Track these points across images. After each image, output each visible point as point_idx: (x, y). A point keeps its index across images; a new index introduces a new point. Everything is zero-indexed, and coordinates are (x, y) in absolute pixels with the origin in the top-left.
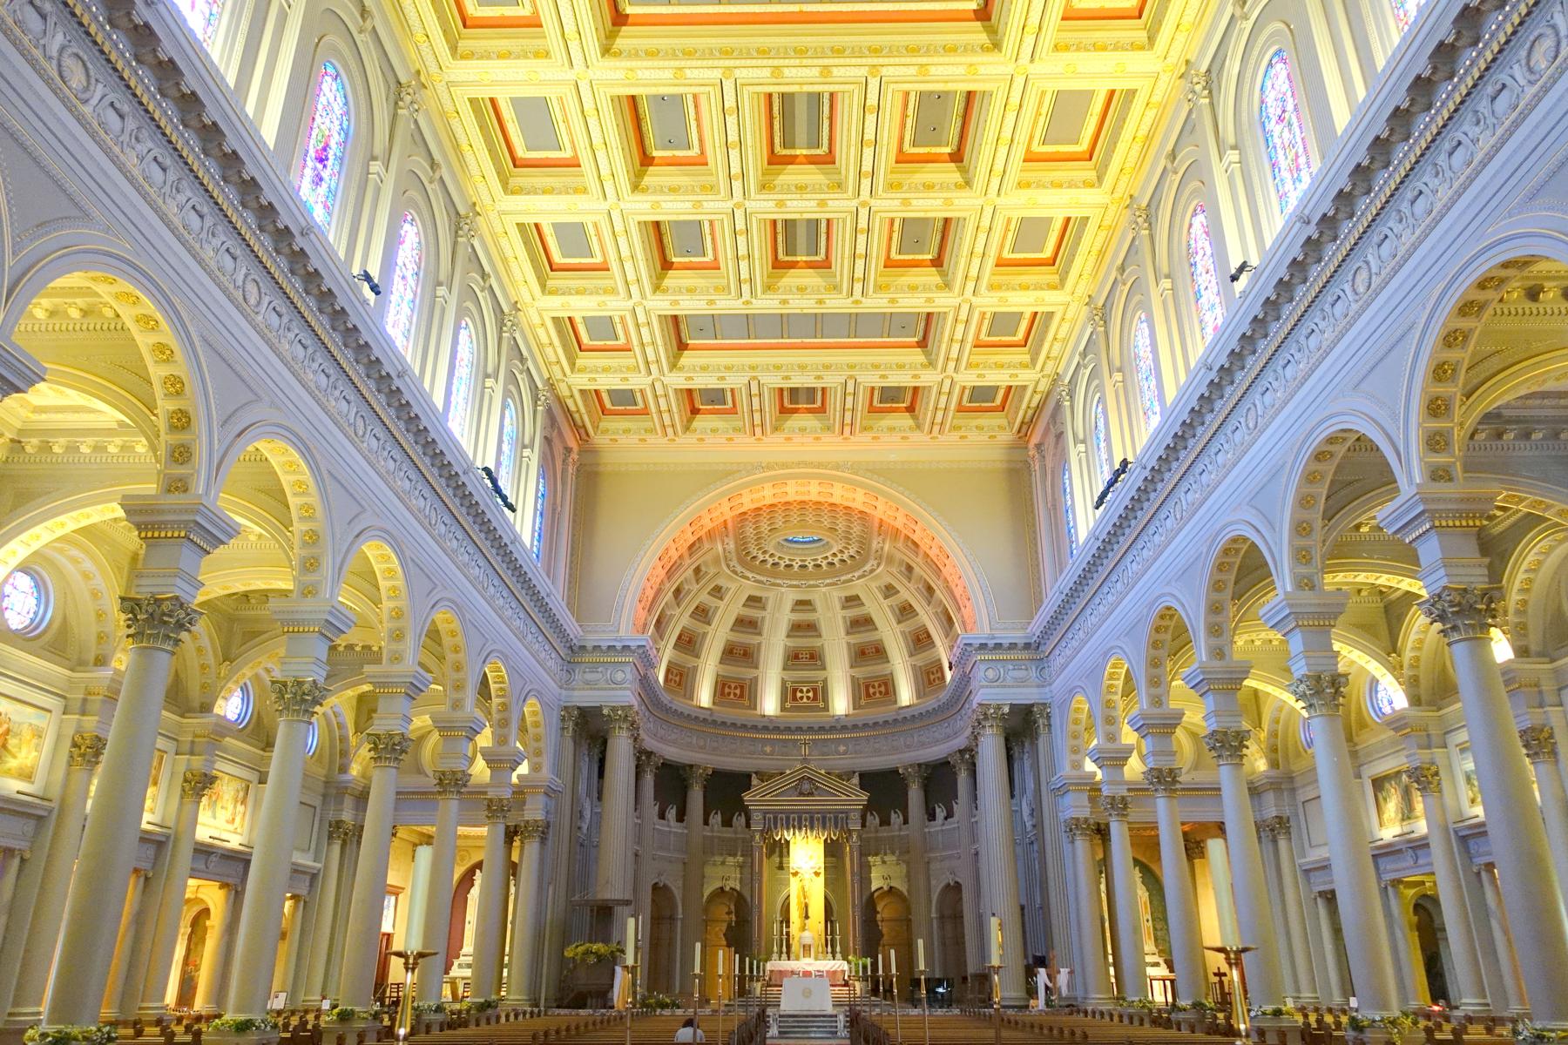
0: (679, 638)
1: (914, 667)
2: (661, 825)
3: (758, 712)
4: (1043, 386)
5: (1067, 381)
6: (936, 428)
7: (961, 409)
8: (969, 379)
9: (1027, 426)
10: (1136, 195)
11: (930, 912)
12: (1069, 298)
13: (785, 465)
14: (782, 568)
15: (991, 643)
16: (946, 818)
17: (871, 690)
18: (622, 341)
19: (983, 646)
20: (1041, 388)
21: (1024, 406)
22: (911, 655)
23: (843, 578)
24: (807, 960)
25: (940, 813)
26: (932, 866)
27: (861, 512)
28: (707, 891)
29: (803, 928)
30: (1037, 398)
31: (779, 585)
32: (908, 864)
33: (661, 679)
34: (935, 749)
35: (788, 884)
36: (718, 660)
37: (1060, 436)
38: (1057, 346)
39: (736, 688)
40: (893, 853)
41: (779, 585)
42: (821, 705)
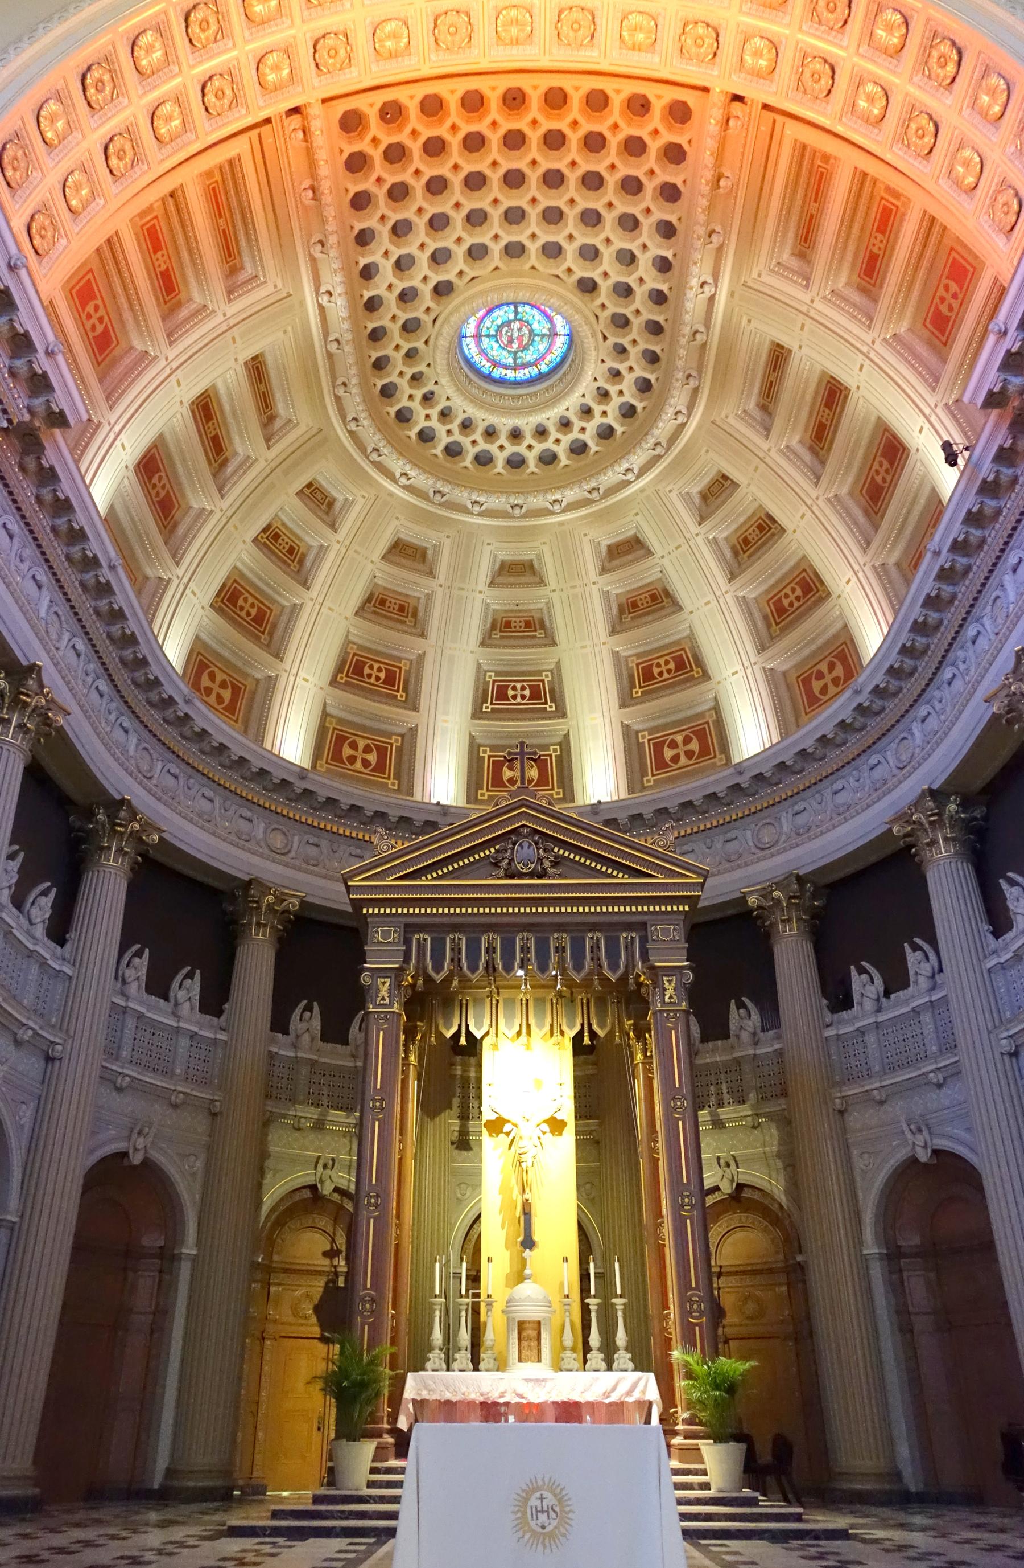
1: (770, 675)
3: (417, 797)
11: (860, 1243)
16: (887, 994)
17: (668, 753)
22: (762, 648)
24: (530, 1369)
26: (854, 1119)
28: (273, 1192)
29: (519, 1276)
32: (785, 1122)
34: (842, 830)
35: (473, 1180)
39: (367, 749)
40: (742, 1101)
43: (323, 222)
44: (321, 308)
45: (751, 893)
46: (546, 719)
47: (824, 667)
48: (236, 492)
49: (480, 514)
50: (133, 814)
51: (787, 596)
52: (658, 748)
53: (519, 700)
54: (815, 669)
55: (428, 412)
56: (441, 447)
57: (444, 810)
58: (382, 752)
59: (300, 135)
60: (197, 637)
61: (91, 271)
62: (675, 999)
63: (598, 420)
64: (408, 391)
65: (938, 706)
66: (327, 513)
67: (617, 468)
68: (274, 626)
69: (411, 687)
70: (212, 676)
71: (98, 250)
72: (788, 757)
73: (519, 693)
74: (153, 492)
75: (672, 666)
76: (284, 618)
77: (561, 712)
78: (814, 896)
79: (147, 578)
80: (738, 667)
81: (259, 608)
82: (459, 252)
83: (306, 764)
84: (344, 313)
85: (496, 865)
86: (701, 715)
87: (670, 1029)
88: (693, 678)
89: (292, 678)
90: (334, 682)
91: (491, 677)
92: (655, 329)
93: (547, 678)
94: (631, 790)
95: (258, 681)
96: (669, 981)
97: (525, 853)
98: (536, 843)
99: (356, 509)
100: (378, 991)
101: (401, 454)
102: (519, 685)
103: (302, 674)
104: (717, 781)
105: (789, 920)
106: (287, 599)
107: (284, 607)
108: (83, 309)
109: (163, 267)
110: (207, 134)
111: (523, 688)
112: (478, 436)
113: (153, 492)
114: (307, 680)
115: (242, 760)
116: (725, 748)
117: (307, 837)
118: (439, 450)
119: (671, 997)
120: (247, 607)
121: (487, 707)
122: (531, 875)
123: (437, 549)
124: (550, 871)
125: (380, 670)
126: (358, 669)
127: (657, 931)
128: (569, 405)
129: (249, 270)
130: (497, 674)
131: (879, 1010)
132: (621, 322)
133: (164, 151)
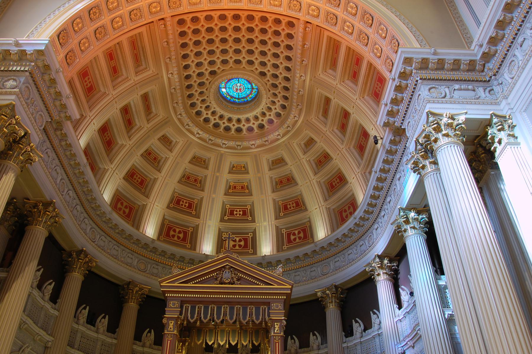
1: (328, 209)
2: (83, 328)
17: (292, 237)
22: (326, 200)
25: (358, 327)
33: (107, 196)
36: (166, 205)
39: (180, 232)
42: (251, 251)
43: (170, 52)
44: (169, 78)
45: (318, 291)
46: (248, 223)
47: (347, 208)
48: (135, 138)
49: (226, 148)
50: (86, 255)
51: (334, 182)
52: (289, 235)
53: (238, 215)
54: (344, 208)
55: (207, 112)
56: (212, 124)
57: (207, 257)
58: (185, 233)
59: (163, 26)
60: (117, 189)
61: (88, 67)
62: (279, 332)
63: (268, 117)
64: (200, 105)
65: (381, 225)
66: (169, 146)
67: (274, 134)
68: (147, 186)
69: (198, 209)
70: (122, 204)
71: (91, 61)
72: (332, 241)
73: (238, 213)
74: (105, 139)
75: (294, 205)
76: (151, 183)
77: (253, 221)
78: (342, 293)
79: (100, 168)
80: (317, 207)
81: (142, 179)
82: (218, 62)
83: (155, 238)
84: (177, 80)
85: (216, 279)
86: (304, 223)
87: (276, 343)
88: (302, 210)
89: (152, 205)
90: (168, 207)
91: (228, 207)
92: (286, 89)
93: (249, 207)
94: (278, 251)
95: (139, 206)
96: (277, 325)
97: (227, 275)
98: (231, 272)
100: (169, 325)
101: (197, 126)
102: (238, 210)
103: (156, 204)
104: (308, 248)
105: (332, 302)
106: (153, 176)
107: (151, 179)
108: (84, 79)
109: (114, 65)
110: (131, 26)
111: (240, 211)
112: (225, 121)
113: (105, 139)
114: (158, 206)
115: (130, 235)
116: (312, 236)
117: (154, 265)
118: (211, 125)
119: (277, 331)
120: (137, 178)
121: (226, 218)
122: (229, 283)
123: (209, 159)
124: (236, 282)
125: (186, 203)
126: (178, 202)
127: (274, 306)
128: (257, 112)
129: (144, 66)
130: (230, 205)
131: (362, 337)
132: (275, 86)
133: (115, 31)
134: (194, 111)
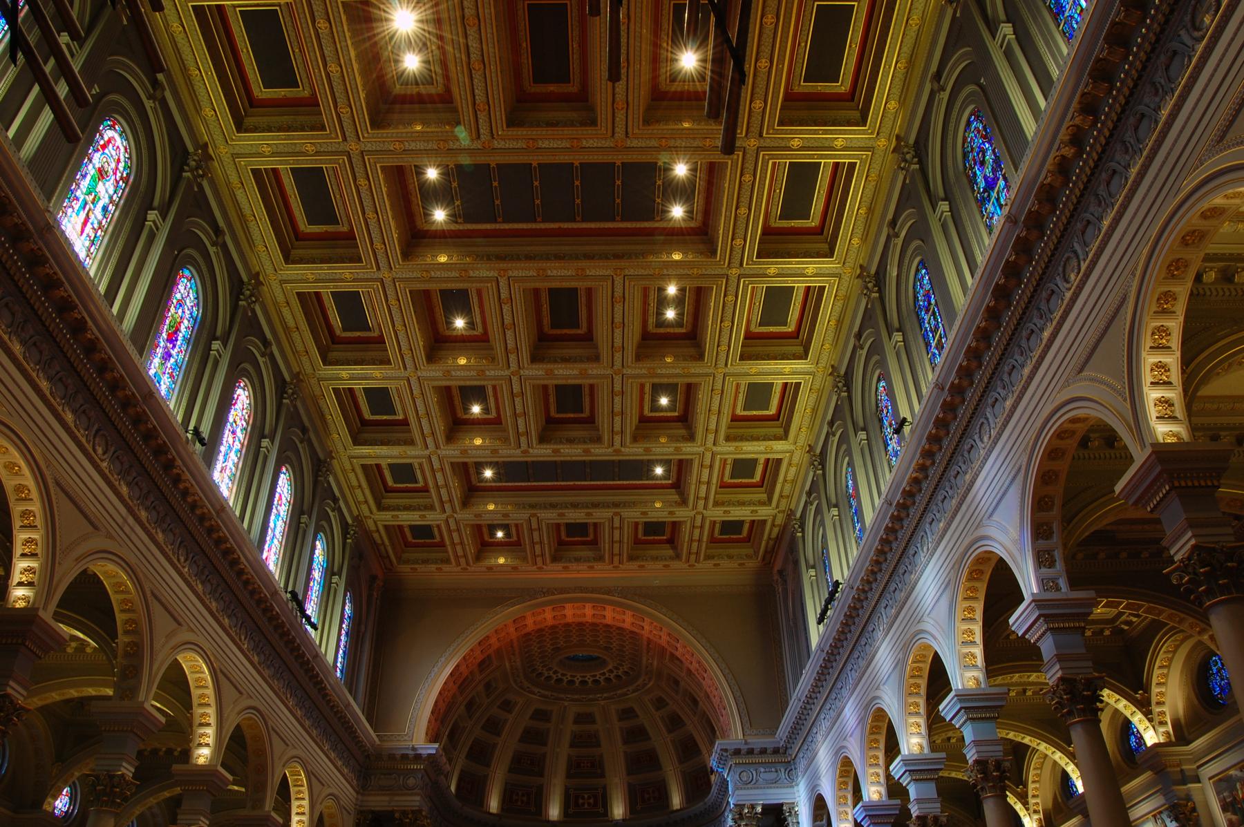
0: (471, 748)
4: (780, 520)
5: (798, 515)
6: (693, 557)
7: (713, 540)
8: (717, 514)
9: (771, 553)
10: (836, 365)
12: (792, 447)
13: (562, 591)
14: (564, 684)
15: (744, 748)
18: (421, 484)
19: (737, 752)
20: (779, 521)
21: (765, 537)
23: (619, 692)
27: (632, 632)
30: (776, 530)
31: (562, 699)
33: (453, 788)
37: (796, 563)
38: (788, 487)
41: (562, 699)
42: (601, 810)
63: (615, 673)
77: (603, 776)
99: (519, 705)
134: (535, 675)
